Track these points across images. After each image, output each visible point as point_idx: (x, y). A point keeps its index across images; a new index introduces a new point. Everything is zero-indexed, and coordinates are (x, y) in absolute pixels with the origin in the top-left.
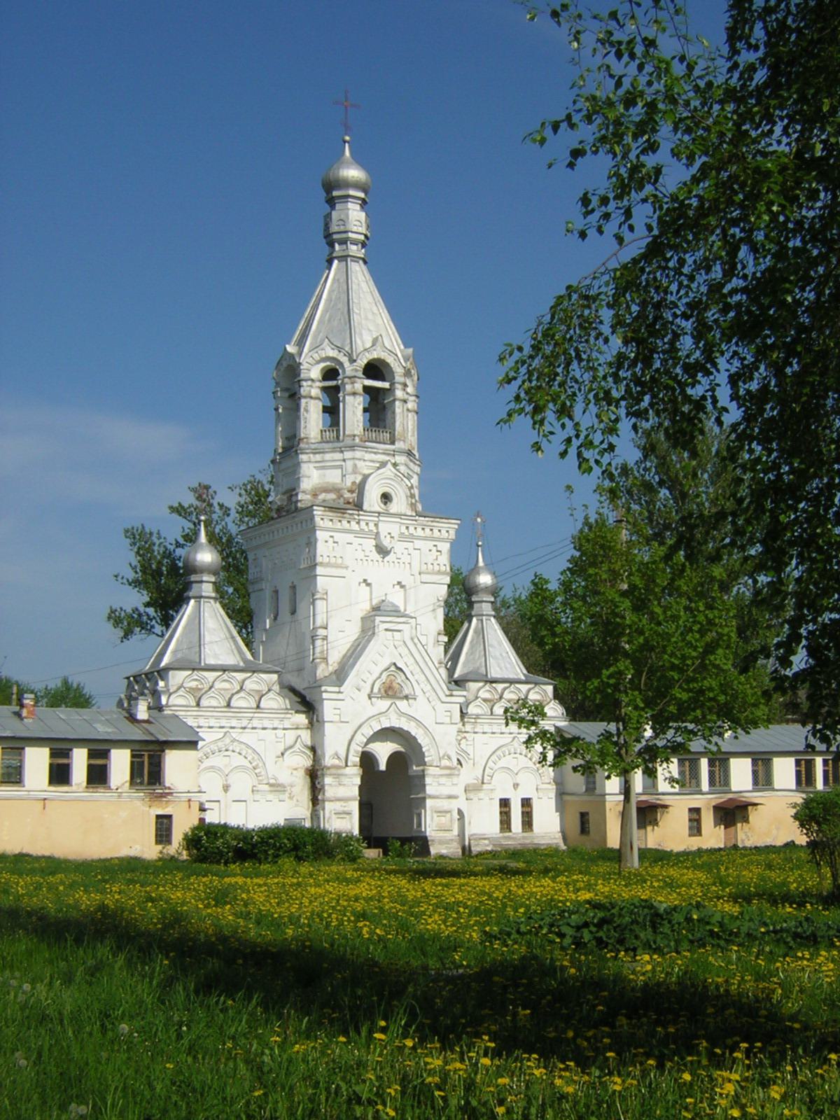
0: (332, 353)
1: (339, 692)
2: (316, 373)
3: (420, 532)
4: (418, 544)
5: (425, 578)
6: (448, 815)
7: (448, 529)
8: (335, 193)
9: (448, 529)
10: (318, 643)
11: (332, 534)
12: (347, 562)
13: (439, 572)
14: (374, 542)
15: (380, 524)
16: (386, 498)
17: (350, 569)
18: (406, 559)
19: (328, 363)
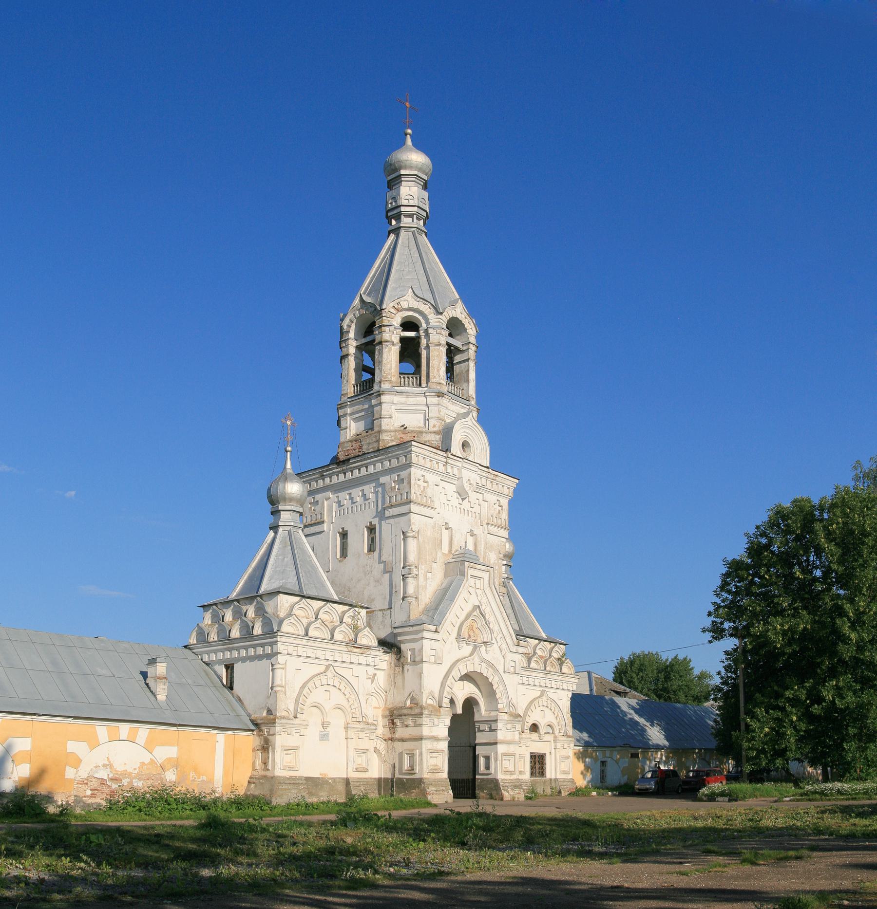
0: (415, 304)
1: (436, 631)
2: (397, 321)
3: (489, 486)
4: (488, 496)
5: (493, 530)
6: (512, 759)
7: (508, 484)
8: (402, 172)
9: (508, 484)
10: (411, 582)
11: (424, 473)
12: (436, 504)
13: (500, 527)
14: (454, 488)
15: (464, 471)
16: (465, 445)
17: (436, 511)
18: (477, 509)
19: (411, 313)
